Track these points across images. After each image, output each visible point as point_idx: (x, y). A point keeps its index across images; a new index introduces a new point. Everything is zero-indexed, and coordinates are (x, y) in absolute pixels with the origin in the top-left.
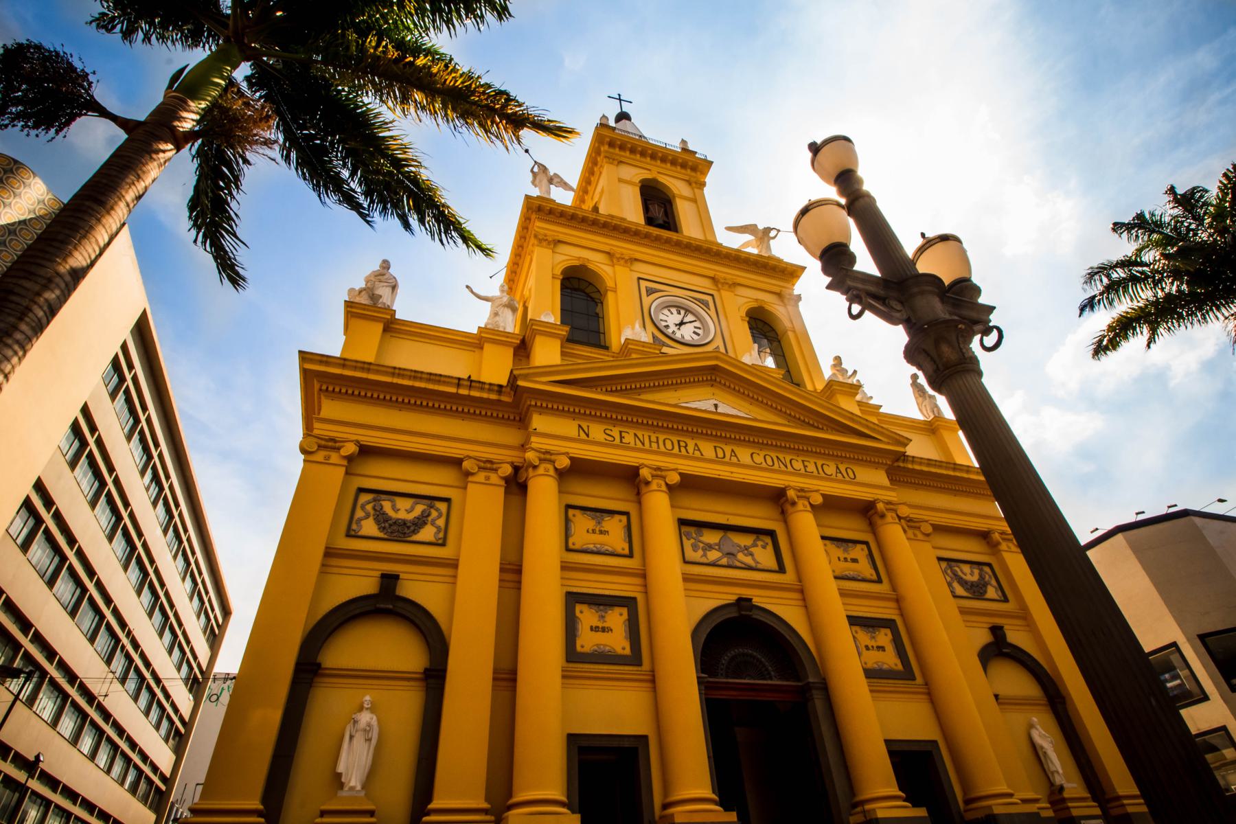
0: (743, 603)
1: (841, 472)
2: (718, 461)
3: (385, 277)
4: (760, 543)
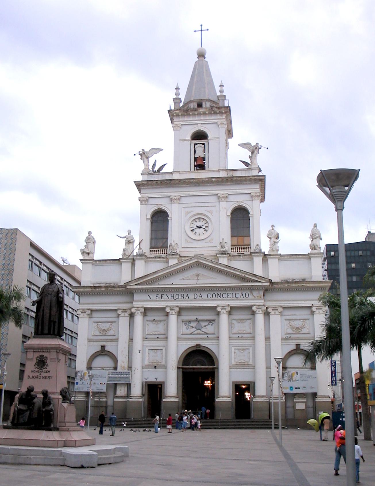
2: (195, 299)
3: (91, 239)
4: (211, 324)
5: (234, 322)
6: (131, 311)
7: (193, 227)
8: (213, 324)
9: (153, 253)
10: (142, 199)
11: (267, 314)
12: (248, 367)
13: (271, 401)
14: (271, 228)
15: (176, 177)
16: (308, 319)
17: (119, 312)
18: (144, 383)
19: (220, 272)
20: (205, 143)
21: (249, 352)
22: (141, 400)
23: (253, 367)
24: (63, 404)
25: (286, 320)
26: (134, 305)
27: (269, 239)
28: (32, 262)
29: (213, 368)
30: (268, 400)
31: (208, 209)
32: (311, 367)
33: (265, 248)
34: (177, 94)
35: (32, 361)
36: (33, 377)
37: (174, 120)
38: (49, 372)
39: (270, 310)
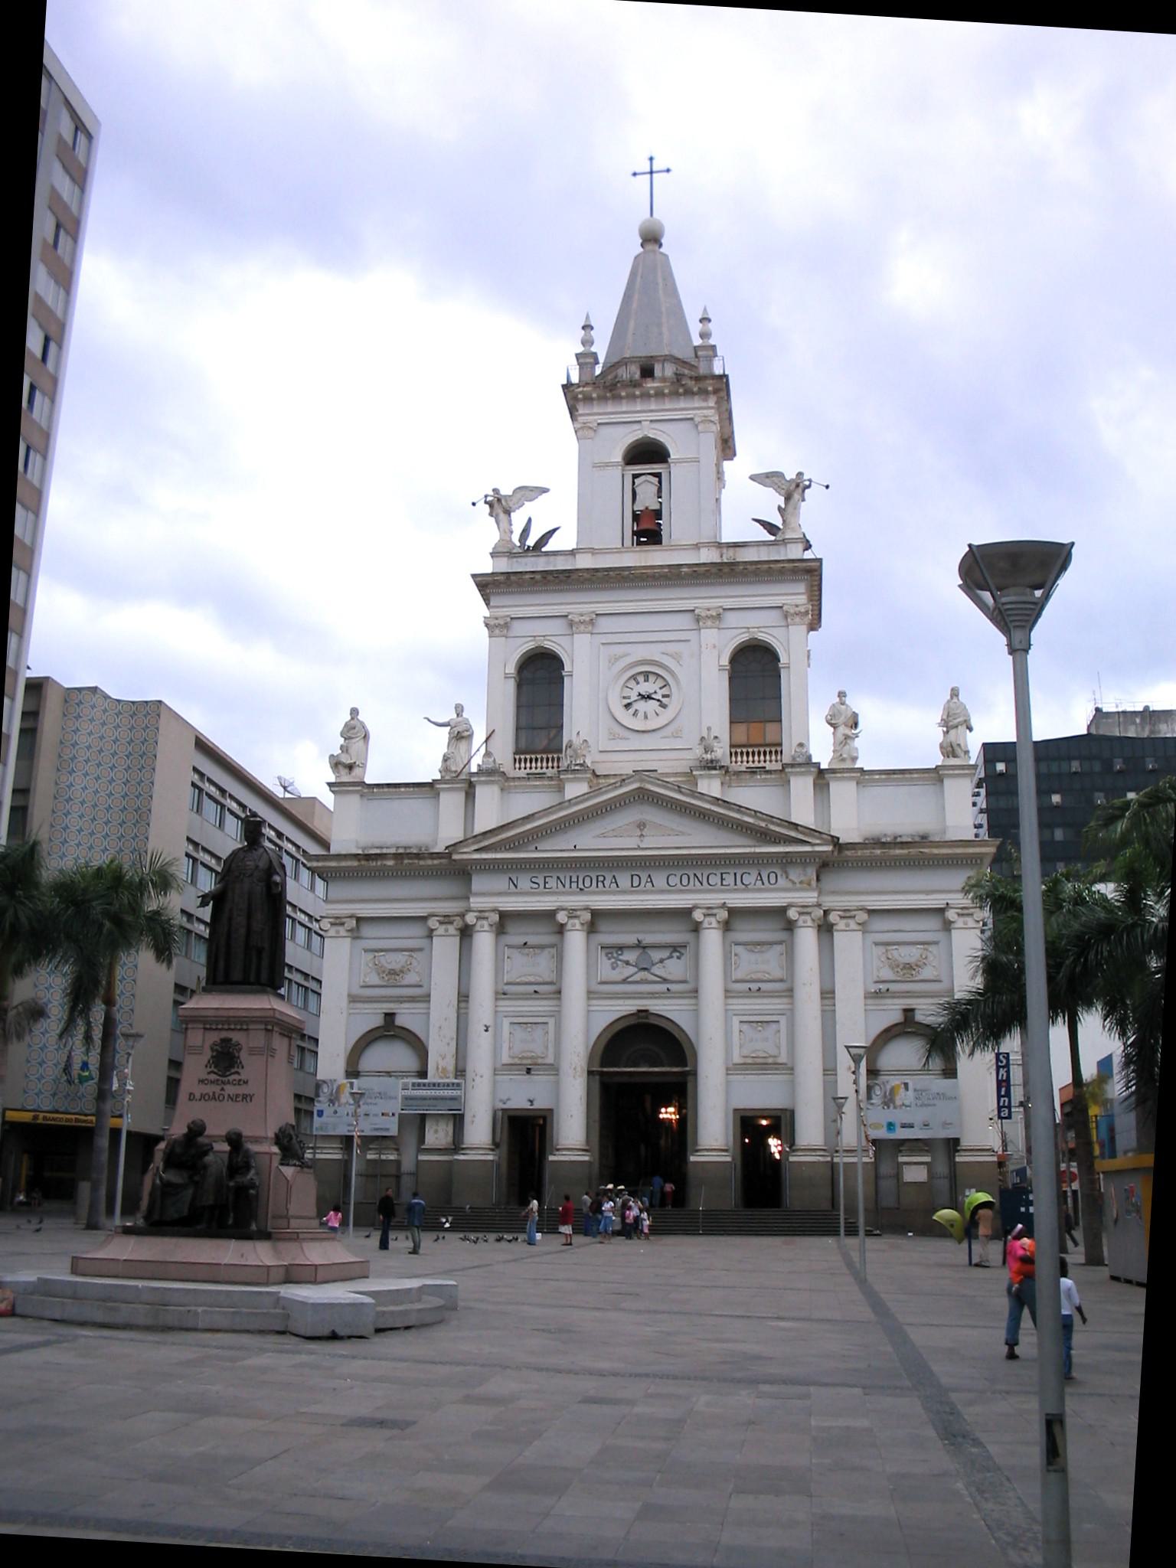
0: (643, 1013)
1: (761, 879)
2: (634, 889)
3: (356, 731)
4: (676, 954)
5: (739, 949)
6: (463, 920)
7: (629, 698)
8: (683, 954)
9: (523, 765)
10: (492, 622)
11: (825, 929)
12: (777, 1069)
13: (836, 1160)
14: (838, 700)
15: (584, 562)
16: (936, 943)
17: (433, 923)
18: (500, 1114)
19: (702, 816)
20: (660, 473)
21: (779, 1031)
22: (490, 1158)
23: (789, 1069)
24: (284, 1169)
25: (876, 944)
26: (472, 905)
27: (832, 729)
28: (201, 790)
29: (684, 1074)
30: (829, 1159)
31: (672, 648)
32: (943, 1070)
33: (822, 753)
34: (587, 342)
35: (200, 1054)
36: (203, 1097)
37: (577, 411)
38: (246, 1082)
39: (833, 917)
